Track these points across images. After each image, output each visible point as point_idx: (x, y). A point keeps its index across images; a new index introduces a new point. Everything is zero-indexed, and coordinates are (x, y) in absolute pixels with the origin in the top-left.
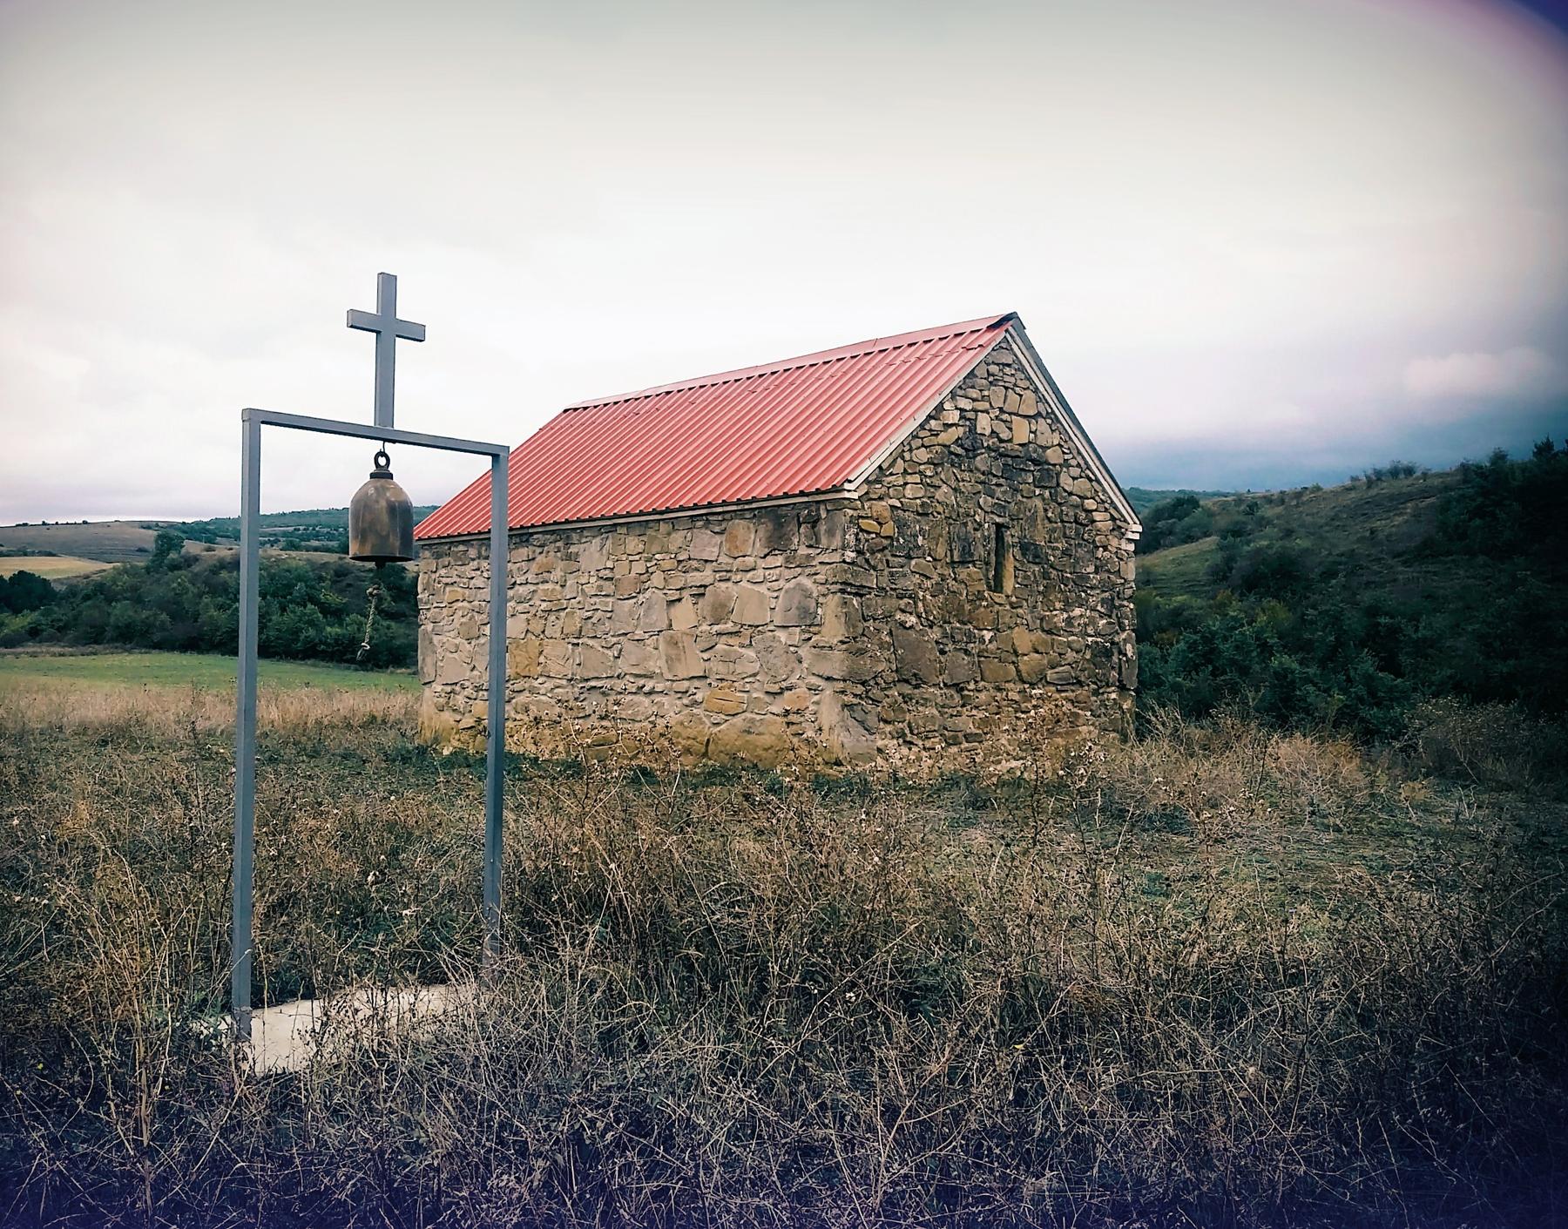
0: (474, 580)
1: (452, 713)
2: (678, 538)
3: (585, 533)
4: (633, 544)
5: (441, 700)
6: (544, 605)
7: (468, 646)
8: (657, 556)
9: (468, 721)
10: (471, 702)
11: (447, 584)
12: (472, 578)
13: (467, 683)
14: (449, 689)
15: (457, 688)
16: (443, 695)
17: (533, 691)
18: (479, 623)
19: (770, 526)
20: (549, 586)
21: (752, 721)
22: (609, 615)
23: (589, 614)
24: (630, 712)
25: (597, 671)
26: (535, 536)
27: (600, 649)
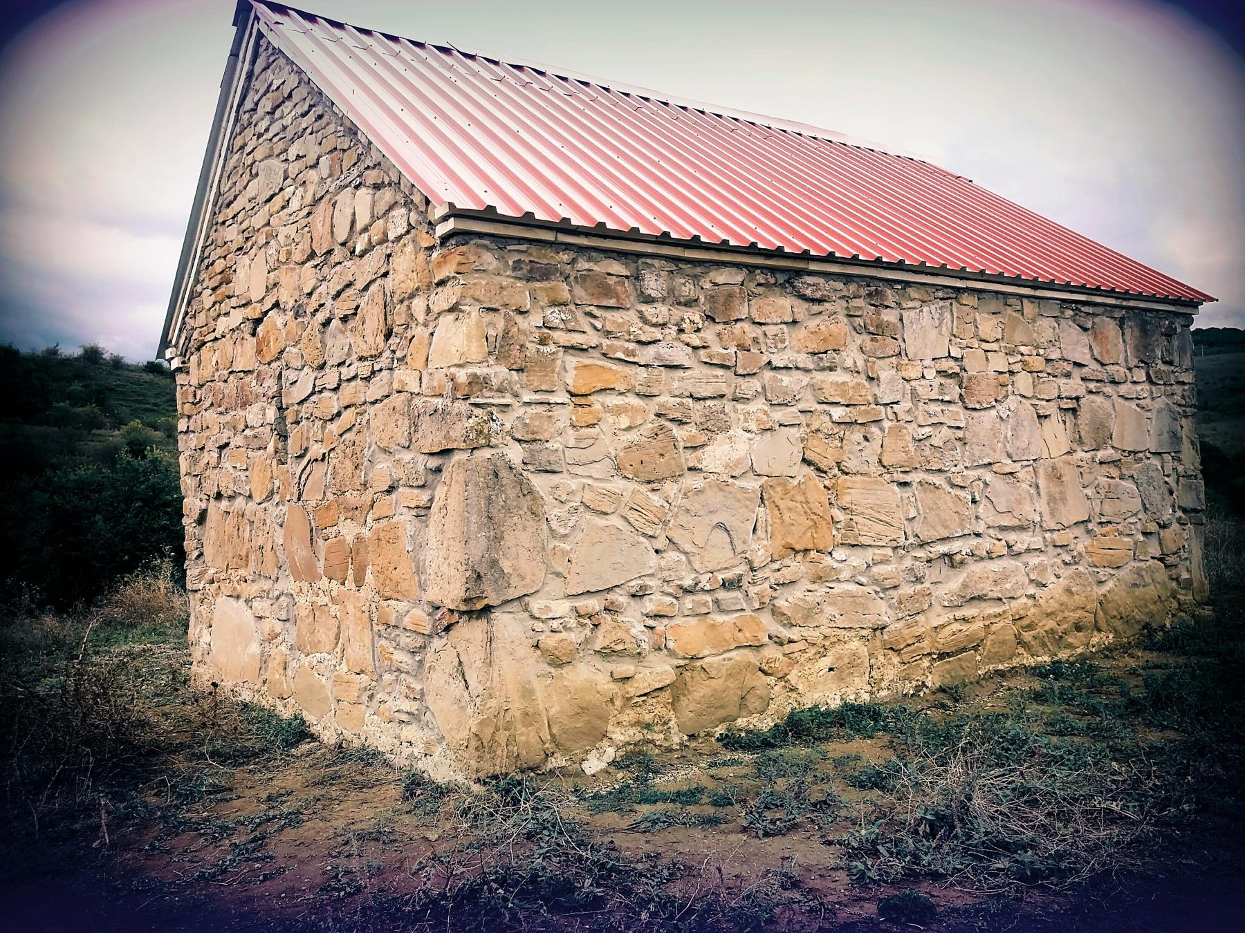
0: (651, 349)
1: (598, 662)
2: (1046, 324)
3: (912, 292)
4: (988, 326)
5: (573, 635)
6: (837, 413)
7: (656, 499)
8: (1022, 349)
9: (660, 670)
10: (660, 625)
11: (568, 348)
12: (654, 342)
13: (649, 582)
14: (594, 604)
15: (620, 598)
16: (572, 622)
17: (818, 579)
18: (681, 445)
19: (1137, 333)
20: (839, 377)
21: (1138, 572)
22: (960, 434)
23: (927, 430)
24: (1008, 586)
25: (946, 527)
26: (810, 280)
27: (951, 490)
